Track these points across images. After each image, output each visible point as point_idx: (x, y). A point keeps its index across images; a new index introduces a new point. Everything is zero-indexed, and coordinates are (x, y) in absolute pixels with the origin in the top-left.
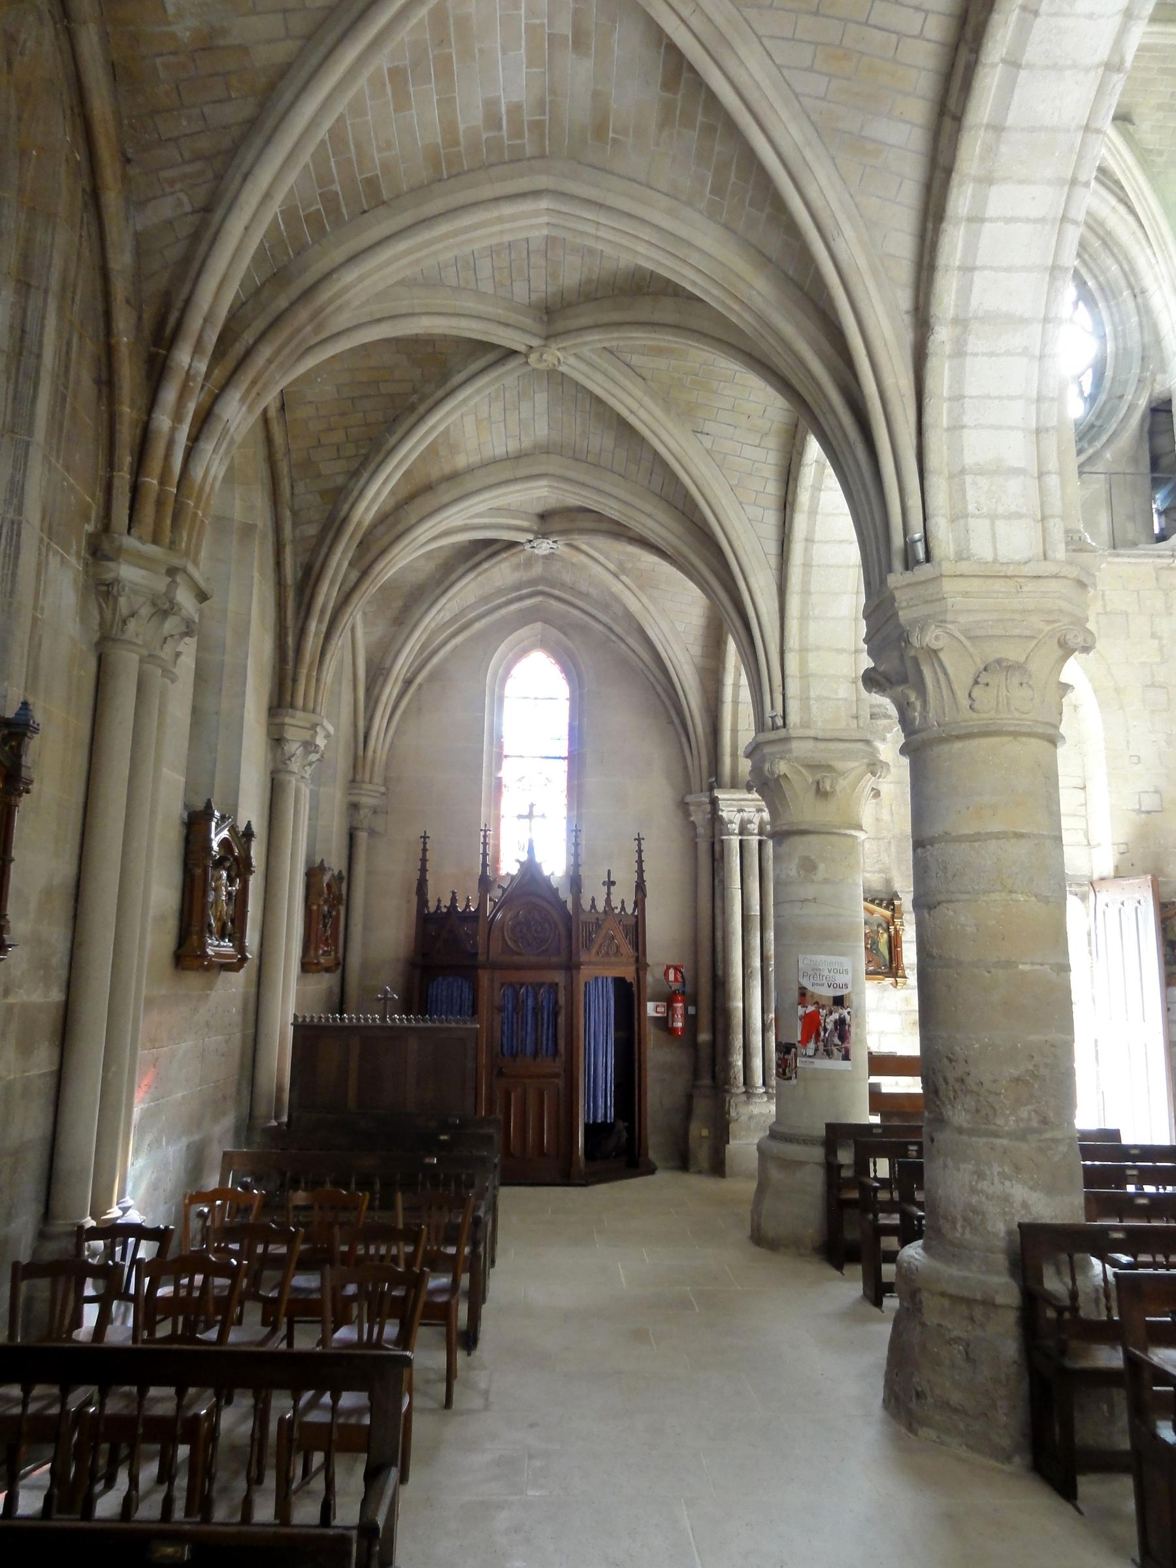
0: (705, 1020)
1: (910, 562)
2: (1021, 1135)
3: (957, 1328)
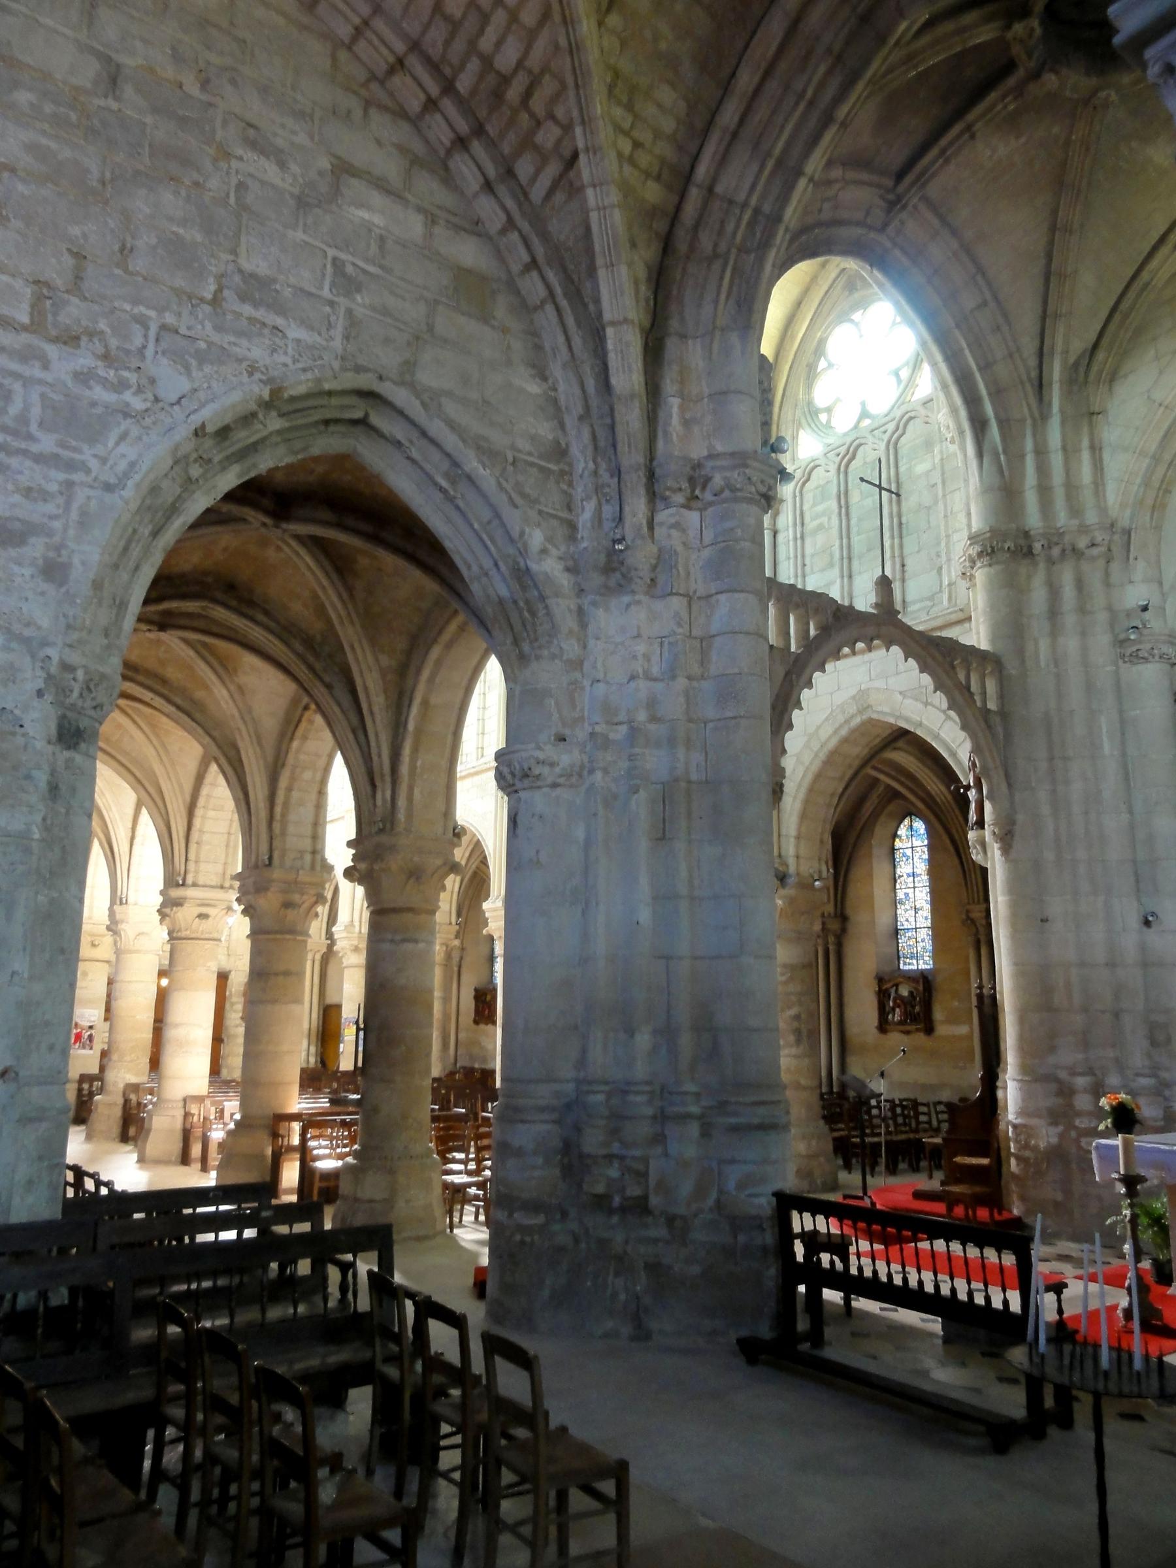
1: (121, 903)
2: (131, 1061)
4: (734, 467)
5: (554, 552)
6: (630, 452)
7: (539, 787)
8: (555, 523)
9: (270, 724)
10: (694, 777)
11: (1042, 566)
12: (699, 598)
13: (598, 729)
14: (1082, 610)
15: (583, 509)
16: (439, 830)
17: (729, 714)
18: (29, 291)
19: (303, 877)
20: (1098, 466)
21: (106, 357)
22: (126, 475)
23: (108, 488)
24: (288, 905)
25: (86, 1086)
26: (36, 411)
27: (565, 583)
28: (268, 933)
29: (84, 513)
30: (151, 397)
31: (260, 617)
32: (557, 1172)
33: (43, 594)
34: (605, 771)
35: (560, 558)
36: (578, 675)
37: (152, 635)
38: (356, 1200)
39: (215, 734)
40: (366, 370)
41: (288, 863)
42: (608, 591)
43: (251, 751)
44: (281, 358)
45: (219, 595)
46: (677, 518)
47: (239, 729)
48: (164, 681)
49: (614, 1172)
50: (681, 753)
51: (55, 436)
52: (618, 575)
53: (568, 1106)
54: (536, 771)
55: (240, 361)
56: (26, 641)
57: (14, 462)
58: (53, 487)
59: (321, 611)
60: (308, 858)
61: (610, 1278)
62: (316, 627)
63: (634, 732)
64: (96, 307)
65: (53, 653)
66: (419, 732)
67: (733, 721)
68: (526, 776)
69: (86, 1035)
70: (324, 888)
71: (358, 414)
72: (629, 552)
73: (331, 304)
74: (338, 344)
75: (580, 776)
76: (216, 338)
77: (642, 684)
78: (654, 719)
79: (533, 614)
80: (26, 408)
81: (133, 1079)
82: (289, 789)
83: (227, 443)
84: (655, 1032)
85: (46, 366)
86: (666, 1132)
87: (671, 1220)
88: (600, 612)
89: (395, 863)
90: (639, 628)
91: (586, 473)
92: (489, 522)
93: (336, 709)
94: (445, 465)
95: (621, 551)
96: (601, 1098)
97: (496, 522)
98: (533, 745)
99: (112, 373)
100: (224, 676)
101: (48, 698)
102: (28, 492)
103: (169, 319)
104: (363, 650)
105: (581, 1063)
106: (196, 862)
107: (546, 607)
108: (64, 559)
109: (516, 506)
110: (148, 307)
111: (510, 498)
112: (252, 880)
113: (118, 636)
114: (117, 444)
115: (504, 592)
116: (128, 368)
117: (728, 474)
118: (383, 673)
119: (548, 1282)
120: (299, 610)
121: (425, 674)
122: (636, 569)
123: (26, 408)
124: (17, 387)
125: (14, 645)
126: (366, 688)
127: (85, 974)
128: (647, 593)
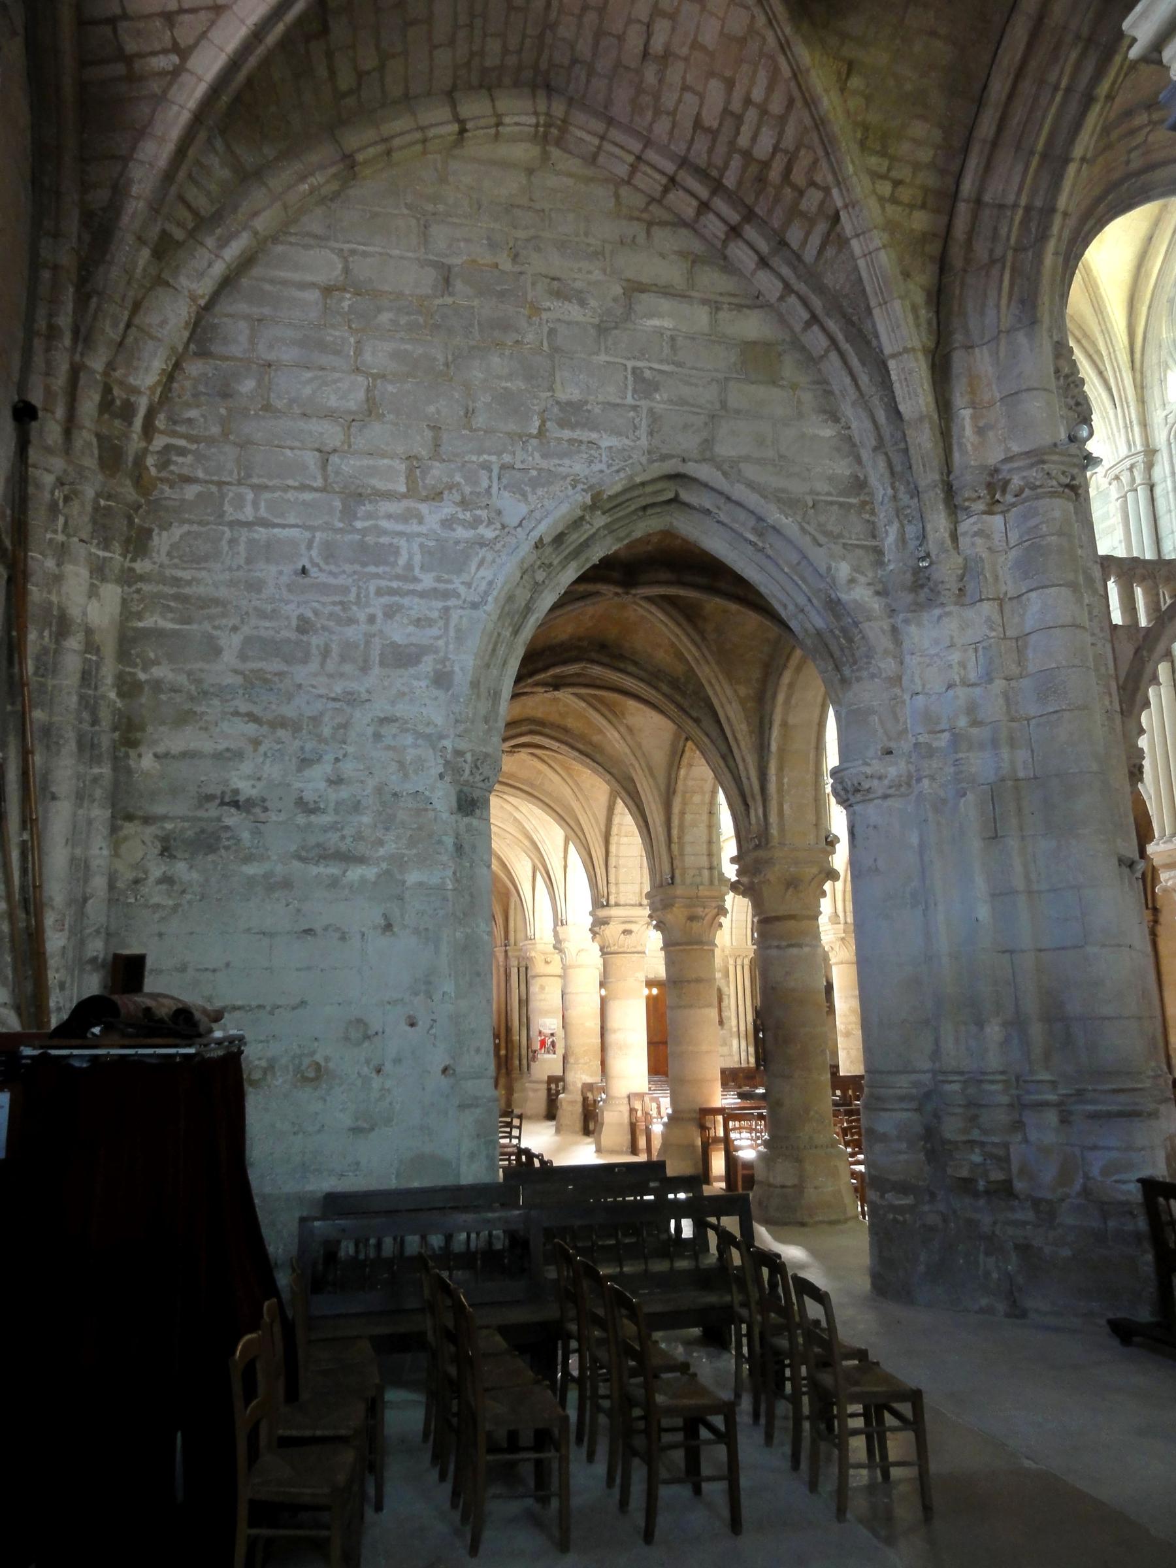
0: (503, 1045)
3: (570, 1108)
4: (1032, 466)
5: (862, 579)
6: (925, 472)
7: (871, 800)
8: (859, 552)
9: (659, 757)
10: (1021, 774)
12: (1010, 599)
13: (921, 739)
15: (887, 532)
16: (811, 839)
17: (1051, 710)
18: (403, 466)
19: (704, 892)
21: (464, 503)
22: (486, 593)
23: (475, 606)
24: (692, 918)
25: (553, 1086)
26: (418, 558)
27: (876, 606)
28: (678, 944)
29: (458, 630)
30: (499, 526)
31: (631, 668)
32: (922, 1156)
33: (436, 699)
34: (932, 778)
35: (869, 584)
36: (897, 691)
37: (548, 695)
38: (770, 1185)
39: (614, 771)
40: (671, 457)
41: (688, 880)
42: (918, 607)
43: (645, 784)
44: (597, 467)
45: (593, 655)
46: (980, 525)
47: (632, 764)
48: (566, 730)
49: (977, 1158)
50: (1005, 753)
51: (434, 574)
52: (926, 590)
53: (928, 1095)
54: (866, 785)
55: (564, 478)
56: (427, 737)
57: (406, 601)
58: (435, 615)
59: (680, 656)
60: (706, 873)
61: (982, 1257)
62: (680, 669)
63: (957, 739)
64: (453, 466)
65: (447, 743)
66: (782, 750)
67: (1055, 716)
68: (857, 791)
69: (549, 1041)
70: (724, 901)
71: (671, 495)
72: (934, 567)
73: (635, 408)
74: (644, 442)
75: (909, 785)
76: (544, 464)
77: (961, 692)
78: (975, 723)
79: (850, 640)
80: (411, 558)
81: (589, 1080)
82: (683, 813)
83: (564, 546)
84: (1005, 1024)
85: (421, 521)
86: (1024, 1119)
87: (1036, 1203)
88: (913, 629)
89: (773, 874)
90: (952, 637)
91: (886, 500)
92: (799, 564)
93: (705, 739)
94: (752, 522)
95: (926, 567)
96: (956, 1087)
97: (804, 563)
98: (860, 762)
99: (468, 514)
100: (613, 719)
101: (448, 779)
102: (417, 622)
103: (507, 458)
104: (722, 687)
105: (936, 1054)
106: (617, 884)
107: (861, 632)
108: (448, 669)
109: (820, 545)
110: (490, 454)
111: (815, 540)
112: (658, 898)
113: (496, 721)
114: (478, 569)
115: (820, 623)
116: (481, 508)
117: (1025, 474)
118: (742, 702)
119: (922, 1259)
120: (662, 657)
121: (781, 698)
122: (942, 582)
123: (411, 558)
124: (403, 543)
125: (420, 742)
126: (728, 719)
127: (542, 988)
128: (956, 604)
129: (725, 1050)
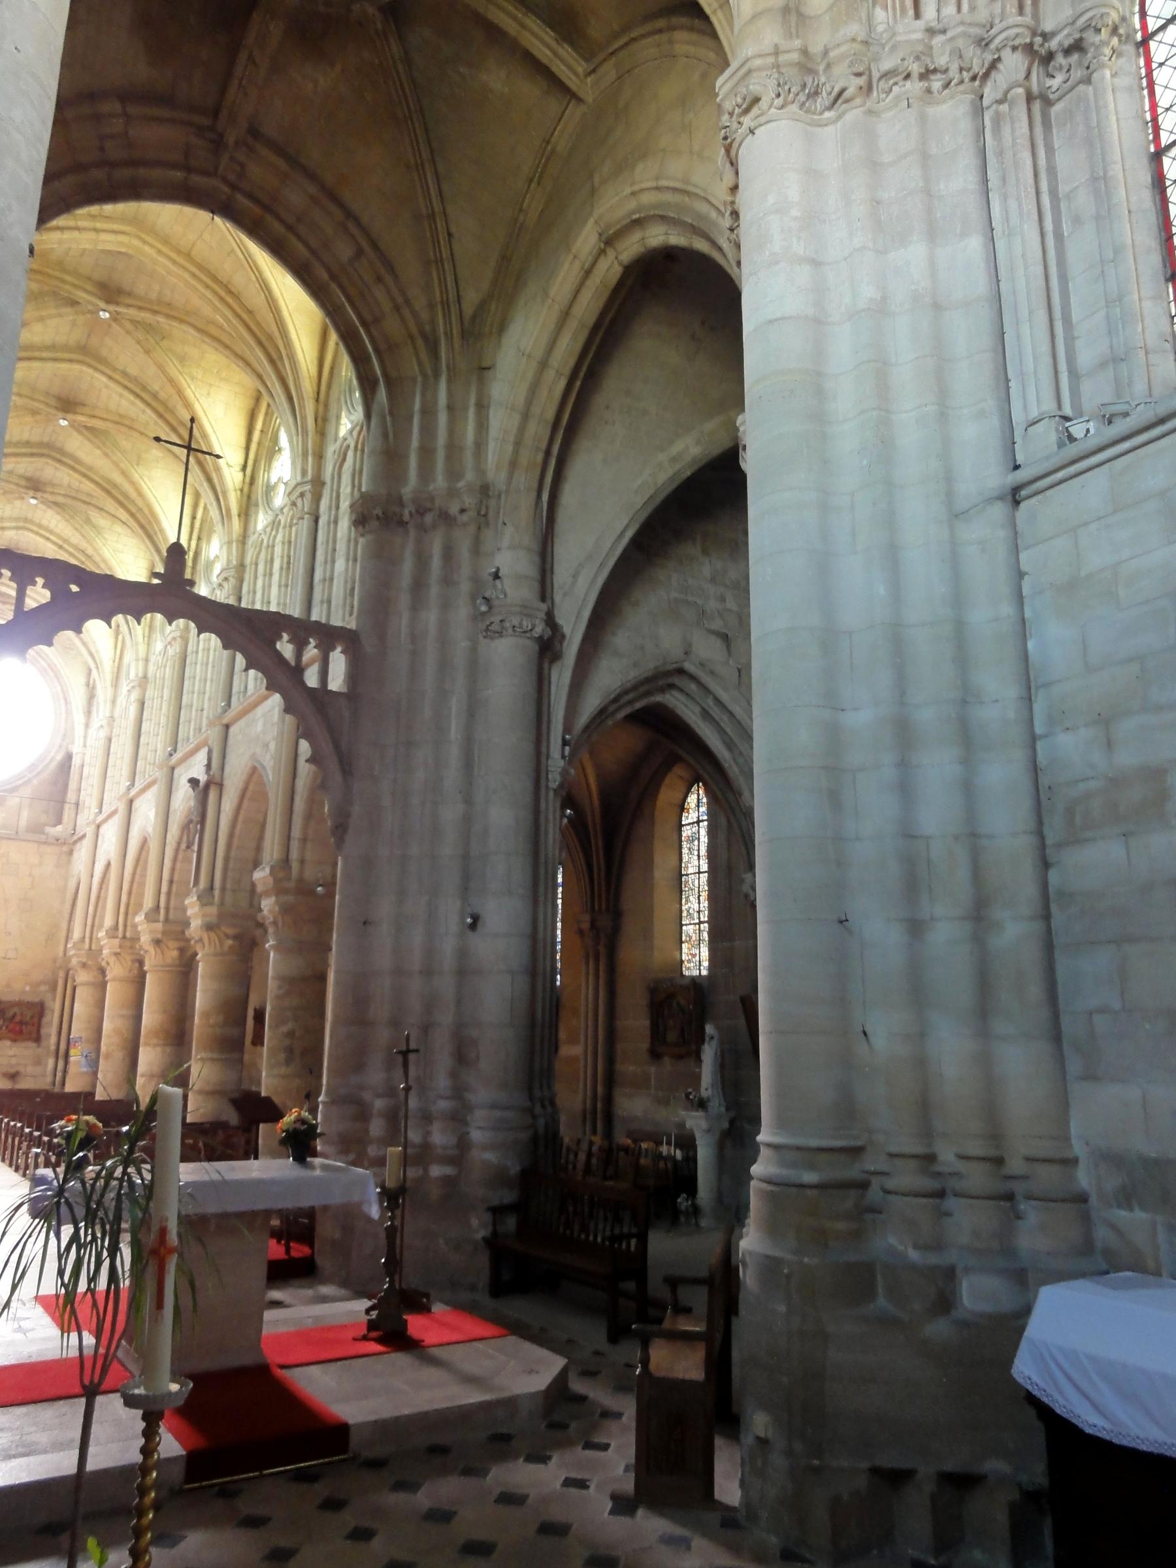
11: (412, 533)
14: (447, 581)
20: (482, 425)
129: (38, 1070)
